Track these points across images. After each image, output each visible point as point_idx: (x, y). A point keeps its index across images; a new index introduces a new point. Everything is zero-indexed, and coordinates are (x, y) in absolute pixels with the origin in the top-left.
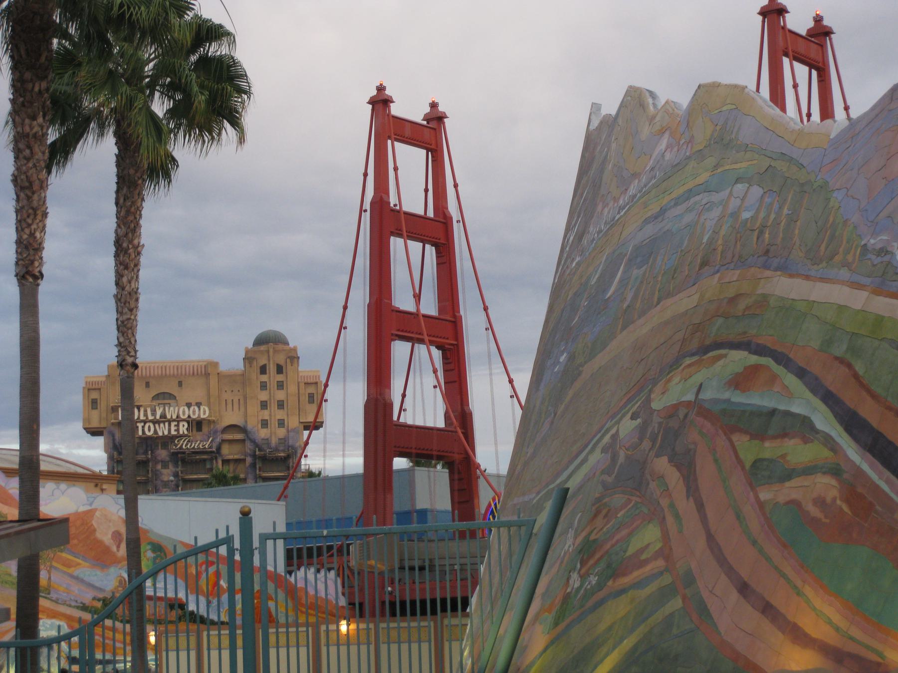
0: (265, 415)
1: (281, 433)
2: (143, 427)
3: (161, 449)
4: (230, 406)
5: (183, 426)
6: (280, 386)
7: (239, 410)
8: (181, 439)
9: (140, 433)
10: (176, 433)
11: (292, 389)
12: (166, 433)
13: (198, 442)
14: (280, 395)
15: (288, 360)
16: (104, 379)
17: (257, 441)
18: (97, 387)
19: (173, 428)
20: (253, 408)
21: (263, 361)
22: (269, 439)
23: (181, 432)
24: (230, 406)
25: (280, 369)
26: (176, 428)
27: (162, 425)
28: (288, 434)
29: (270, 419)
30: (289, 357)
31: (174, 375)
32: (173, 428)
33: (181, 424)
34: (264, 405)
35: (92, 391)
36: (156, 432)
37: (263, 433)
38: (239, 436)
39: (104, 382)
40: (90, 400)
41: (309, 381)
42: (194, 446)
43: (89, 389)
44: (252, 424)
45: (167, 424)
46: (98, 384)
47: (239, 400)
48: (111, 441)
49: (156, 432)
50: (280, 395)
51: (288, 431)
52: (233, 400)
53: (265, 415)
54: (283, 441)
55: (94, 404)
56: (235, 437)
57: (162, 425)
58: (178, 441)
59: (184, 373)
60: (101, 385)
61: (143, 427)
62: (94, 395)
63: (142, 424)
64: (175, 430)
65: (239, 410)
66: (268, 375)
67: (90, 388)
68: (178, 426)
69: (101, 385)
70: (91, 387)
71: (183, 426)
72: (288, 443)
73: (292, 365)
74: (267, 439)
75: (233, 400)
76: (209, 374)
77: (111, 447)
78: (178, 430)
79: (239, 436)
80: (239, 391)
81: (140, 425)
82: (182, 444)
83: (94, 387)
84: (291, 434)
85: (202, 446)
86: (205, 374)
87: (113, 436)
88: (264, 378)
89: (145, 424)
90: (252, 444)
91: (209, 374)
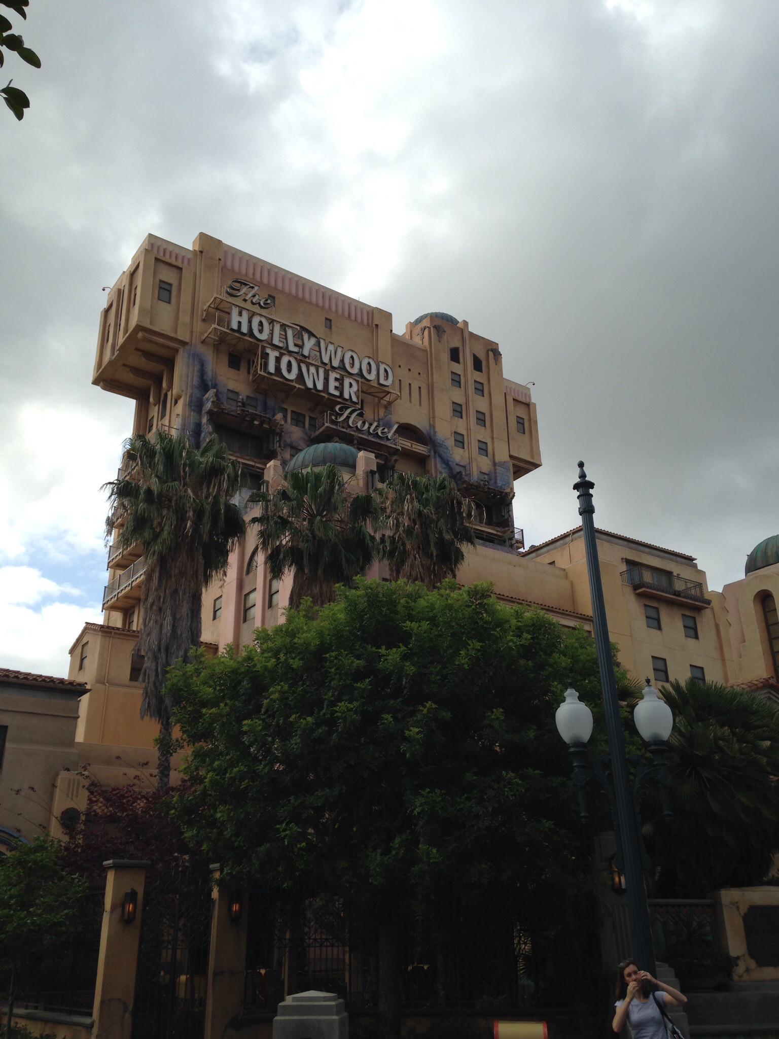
0: (461, 426)
1: (484, 464)
2: (278, 360)
3: (291, 424)
4: (405, 391)
5: (351, 385)
6: (480, 389)
7: (420, 405)
8: (347, 408)
9: (272, 368)
10: (337, 393)
11: (498, 399)
12: (320, 386)
13: (375, 424)
14: (481, 404)
15: (491, 354)
16: (190, 256)
17: (450, 463)
18: (173, 261)
19: (332, 384)
20: (443, 409)
21: (456, 343)
22: (467, 467)
23: (346, 396)
24: (405, 391)
25: (478, 365)
26: (337, 384)
27: (313, 370)
28: (495, 470)
29: (469, 435)
30: (492, 350)
31: (317, 305)
32: (332, 384)
33: (347, 381)
34: (458, 411)
35: (162, 266)
36: (300, 377)
37: (458, 455)
38: (420, 449)
39: (189, 260)
40: (158, 282)
41: (520, 399)
42: (369, 428)
43: (156, 259)
44: (444, 431)
45: (321, 371)
46: (176, 258)
47: (420, 388)
48: (196, 373)
49: (300, 377)
50: (481, 404)
51: (495, 464)
52: (410, 384)
53: (461, 426)
54: (491, 476)
55: (164, 291)
56: (414, 446)
57: (313, 370)
58: (341, 409)
59: (334, 309)
60: (183, 262)
61: (278, 360)
62: (168, 275)
63: (277, 354)
64: (336, 388)
65: (420, 405)
66: (462, 365)
67: (159, 257)
68: (340, 380)
69: (183, 262)
70: (161, 256)
71: (351, 385)
72: (496, 483)
73: (496, 364)
74: (465, 467)
75: (410, 384)
76: (377, 325)
77: (195, 383)
78: (340, 389)
79: (420, 449)
80: (419, 374)
81: (273, 354)
82: (348, 417)
83: (167, 259)
84: (500, 470)
85: (382, 433)
86: (368, 325)
87: (202, 364)
88: (457, 368)
89: (282, 355)
90: (444, 466)
91: (377, 325)
